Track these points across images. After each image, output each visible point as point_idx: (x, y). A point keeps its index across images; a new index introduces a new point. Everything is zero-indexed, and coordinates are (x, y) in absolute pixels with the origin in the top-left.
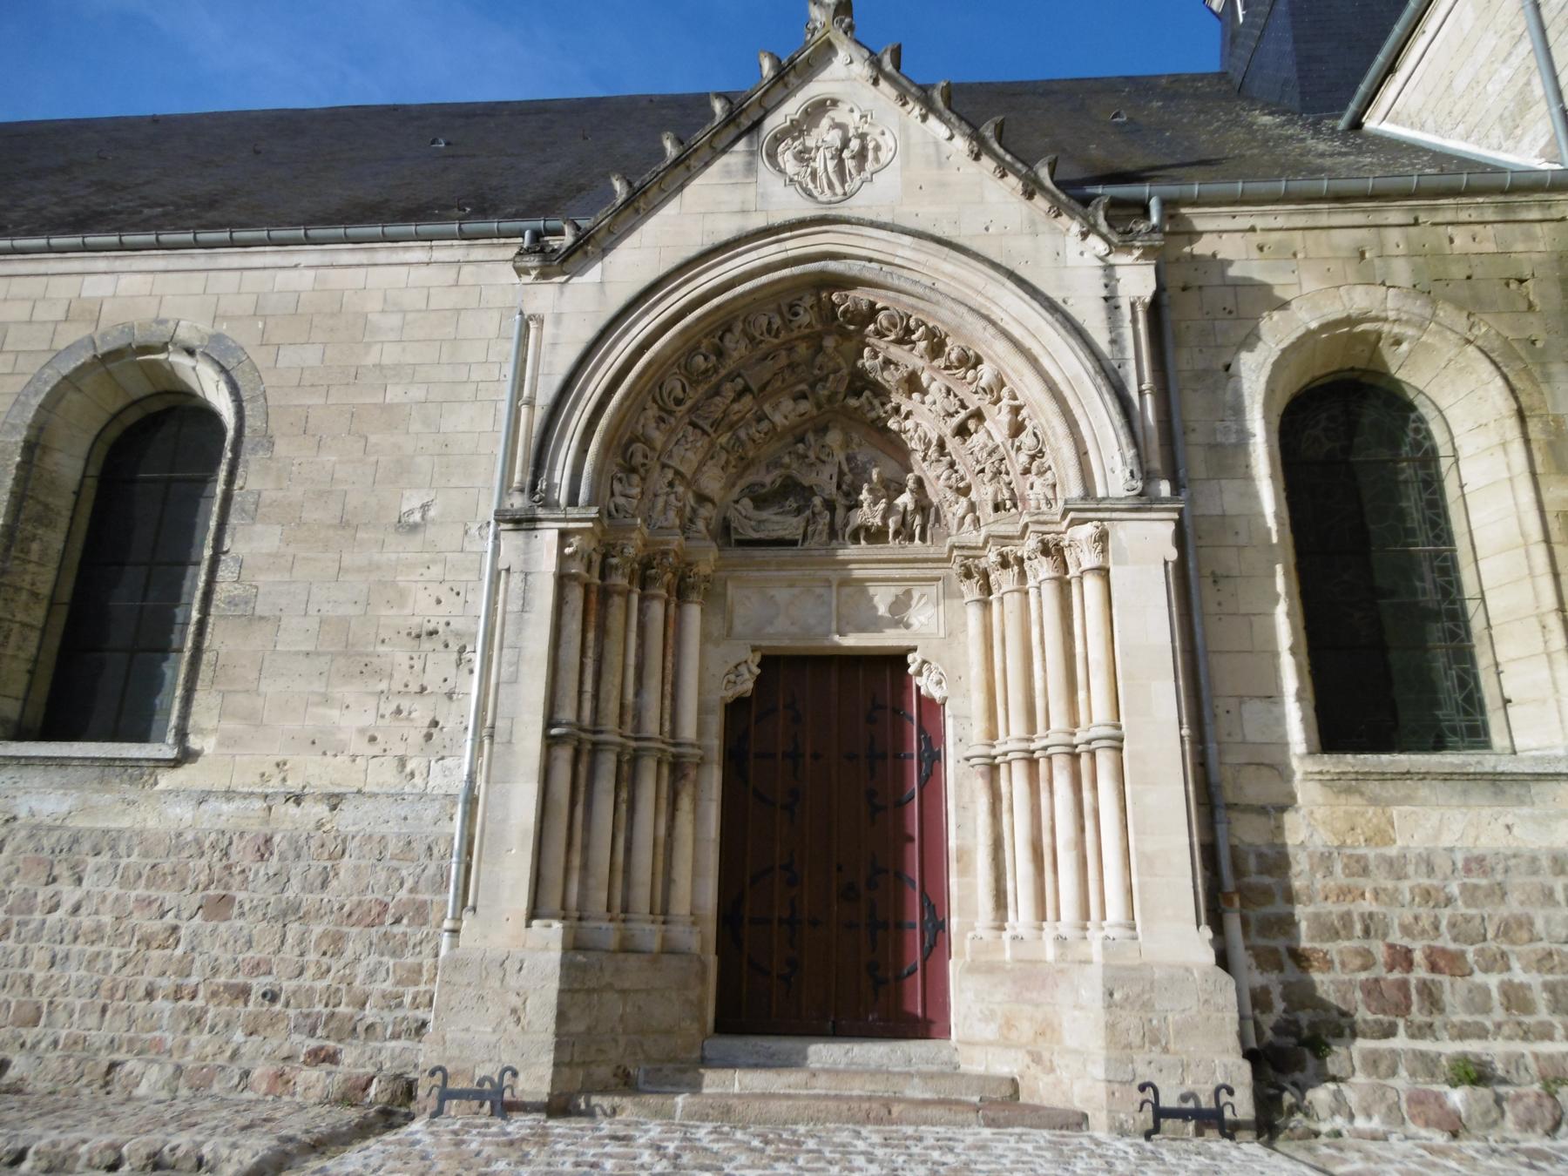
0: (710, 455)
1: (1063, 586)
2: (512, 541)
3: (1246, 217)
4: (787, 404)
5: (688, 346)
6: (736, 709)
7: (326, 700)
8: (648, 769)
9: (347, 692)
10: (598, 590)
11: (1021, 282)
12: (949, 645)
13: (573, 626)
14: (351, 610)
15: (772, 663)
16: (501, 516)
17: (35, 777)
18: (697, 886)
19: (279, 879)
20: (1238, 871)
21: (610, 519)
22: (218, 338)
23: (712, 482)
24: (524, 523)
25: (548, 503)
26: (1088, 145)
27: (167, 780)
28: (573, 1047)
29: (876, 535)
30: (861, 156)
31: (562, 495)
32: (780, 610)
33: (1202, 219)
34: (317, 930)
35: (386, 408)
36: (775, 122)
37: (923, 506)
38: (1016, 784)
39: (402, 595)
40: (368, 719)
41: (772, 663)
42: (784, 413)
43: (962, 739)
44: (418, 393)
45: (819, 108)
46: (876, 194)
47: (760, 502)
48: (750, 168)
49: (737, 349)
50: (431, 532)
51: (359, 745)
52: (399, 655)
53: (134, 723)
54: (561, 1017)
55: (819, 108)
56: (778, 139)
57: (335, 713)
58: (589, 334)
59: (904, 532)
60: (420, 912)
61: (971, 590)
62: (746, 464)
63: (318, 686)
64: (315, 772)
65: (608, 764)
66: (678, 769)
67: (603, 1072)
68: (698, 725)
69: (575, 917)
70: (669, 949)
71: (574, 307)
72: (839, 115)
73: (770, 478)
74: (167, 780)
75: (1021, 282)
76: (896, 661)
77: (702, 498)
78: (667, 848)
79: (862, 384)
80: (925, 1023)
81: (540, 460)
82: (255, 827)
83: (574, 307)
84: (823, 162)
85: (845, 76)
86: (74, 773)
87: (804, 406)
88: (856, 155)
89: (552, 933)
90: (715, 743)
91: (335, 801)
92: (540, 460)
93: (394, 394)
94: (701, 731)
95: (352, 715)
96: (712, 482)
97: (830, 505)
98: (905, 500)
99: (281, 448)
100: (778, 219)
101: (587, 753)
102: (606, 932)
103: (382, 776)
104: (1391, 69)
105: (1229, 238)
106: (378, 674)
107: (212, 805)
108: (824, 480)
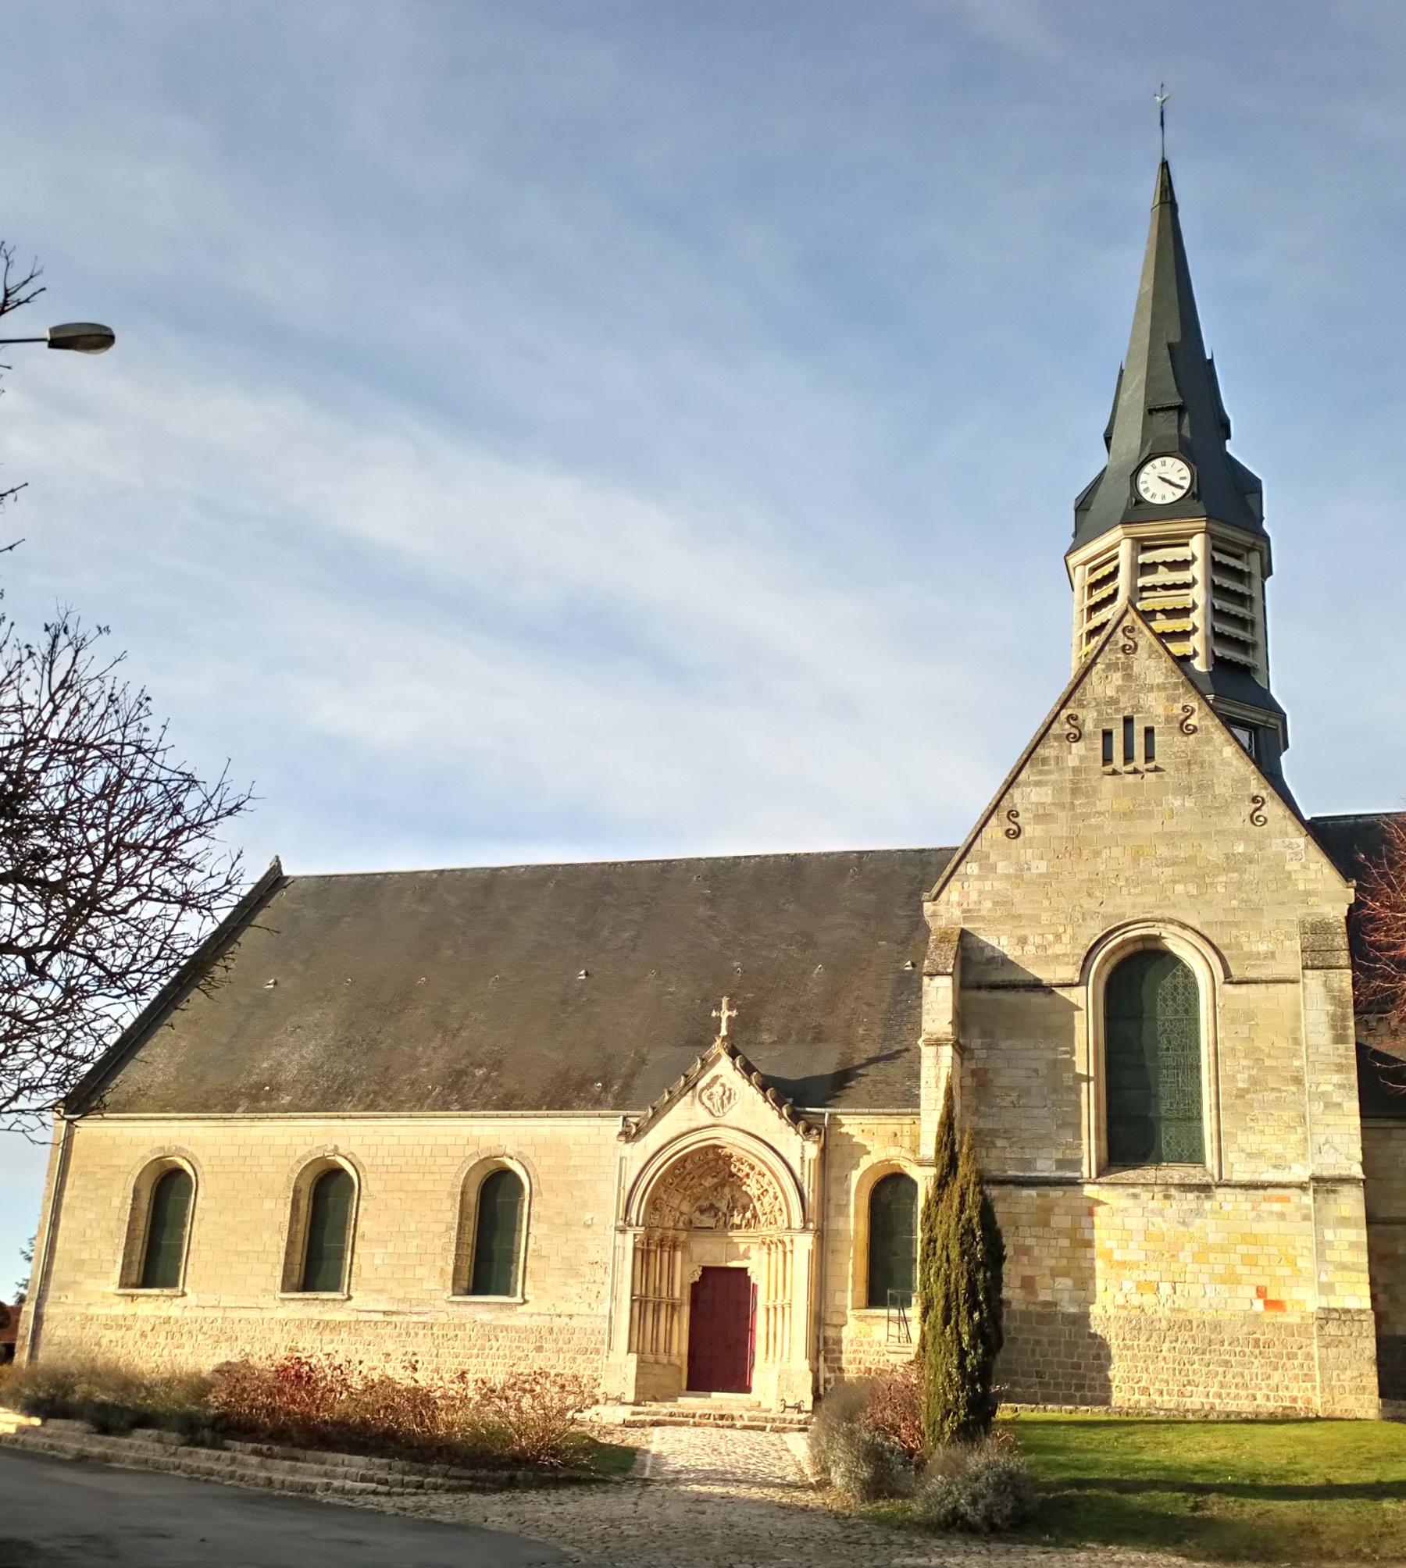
0: (684, 1198)
1: (785, 1253)
2: (619, 1236)
3: (859, 1119)
4: (710, 1179)
5: (674, 1166)
6: (694, 1285)
7: (566, 1284)
8: (663, 1306)
10: (644, 1253)
11: (772, 1148)
12: (759, 1267)
13: (638, 1264)
15: (705, 1269)
16: (616, 1229)
18: (681, 1344)
20: (825, 1343)
21: (649, 1228)
23: (685, 1208)
24: (623, 1231)
25: (630, 1225)
26: (799, 1098)
27: (520, 1309)
28: (640, 1389)
29: (739, 1227)
30: (729, 1098)
31: (634, 1222)
32: (709, 1252)
33: (844, 1119)
35: (578, 1182)
36: (701, 1084)
37: (755, 1216)
38: (779, 1310)
41: (705, 1269)
42: (708, 1182)
43: (762, 1300)
45: (716, 1078)
46: (733, 1115)
47: (702, 1211)
48: (693, 1103)
49: (689, 1165)
51: (577, 1299)
53: (506, 1289)
54: (637, 1380)
55: (716, 1078)
56: (703, 1090)
57: (568, 1288)
58: (641, 1165)
59: (748, 1225)
60: (597, 1351)
61: (765, 1248)
62: (698, 1199)
65: (650, 1307)
66: (674, 1307)
67: (649, 1396)
68: (680, 1292)
69: (640, 1353)
70: (670, 1363)
71: (638, 1153)
72: (721, 1080)
73: (706, 1204)
75: (772, 1148)
76: (744, 1270)
77: (682, 1214)
78: (669, 1333)
79: (732, 1175)
80: (746, 1389)
81: (627, 1210)
83: (638, 1153)
84: (716, 1099)
85: (725, 1069)
87: (716, 1180)
88: (728, 1096)
89: (634, 1357)
90: (686, 1297)
91: (571, 1316)
92: (627, 1210)
94: (681, 1293)
96: (685, 1208)
97: (725, 1215)
98: (748, 1215)
100: (701, 1124)
101: (642, 1303)
102: (651, 1358)
105: (854, 1124)
108: (723, 1205)
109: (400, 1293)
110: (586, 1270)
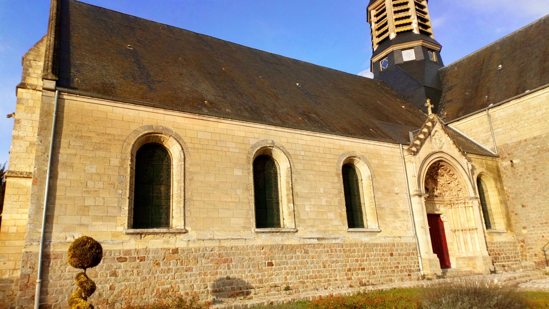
7: (394, 222)
9: (396, 220)
14: (392, 207)
17: (362, 234)
19: (397, 250)
22: (363, 156)
34: (404, 257)
39: (399, 206)
40: (400, 225)
44: (392, 170)
50: (399, 195)
52: (401, 215)
63: (393, 219)
64: (396, 233)
74: (379, 235)
82: (392, 242)
86: (366, 234)
93: (389, 170)
95: (398, 224)
99: (377, 178)
103: (402, 234)
104: (458, 121)
106: (399, 217)
107: (387, 238)
109: (322, 227)
110: (400, 214)
